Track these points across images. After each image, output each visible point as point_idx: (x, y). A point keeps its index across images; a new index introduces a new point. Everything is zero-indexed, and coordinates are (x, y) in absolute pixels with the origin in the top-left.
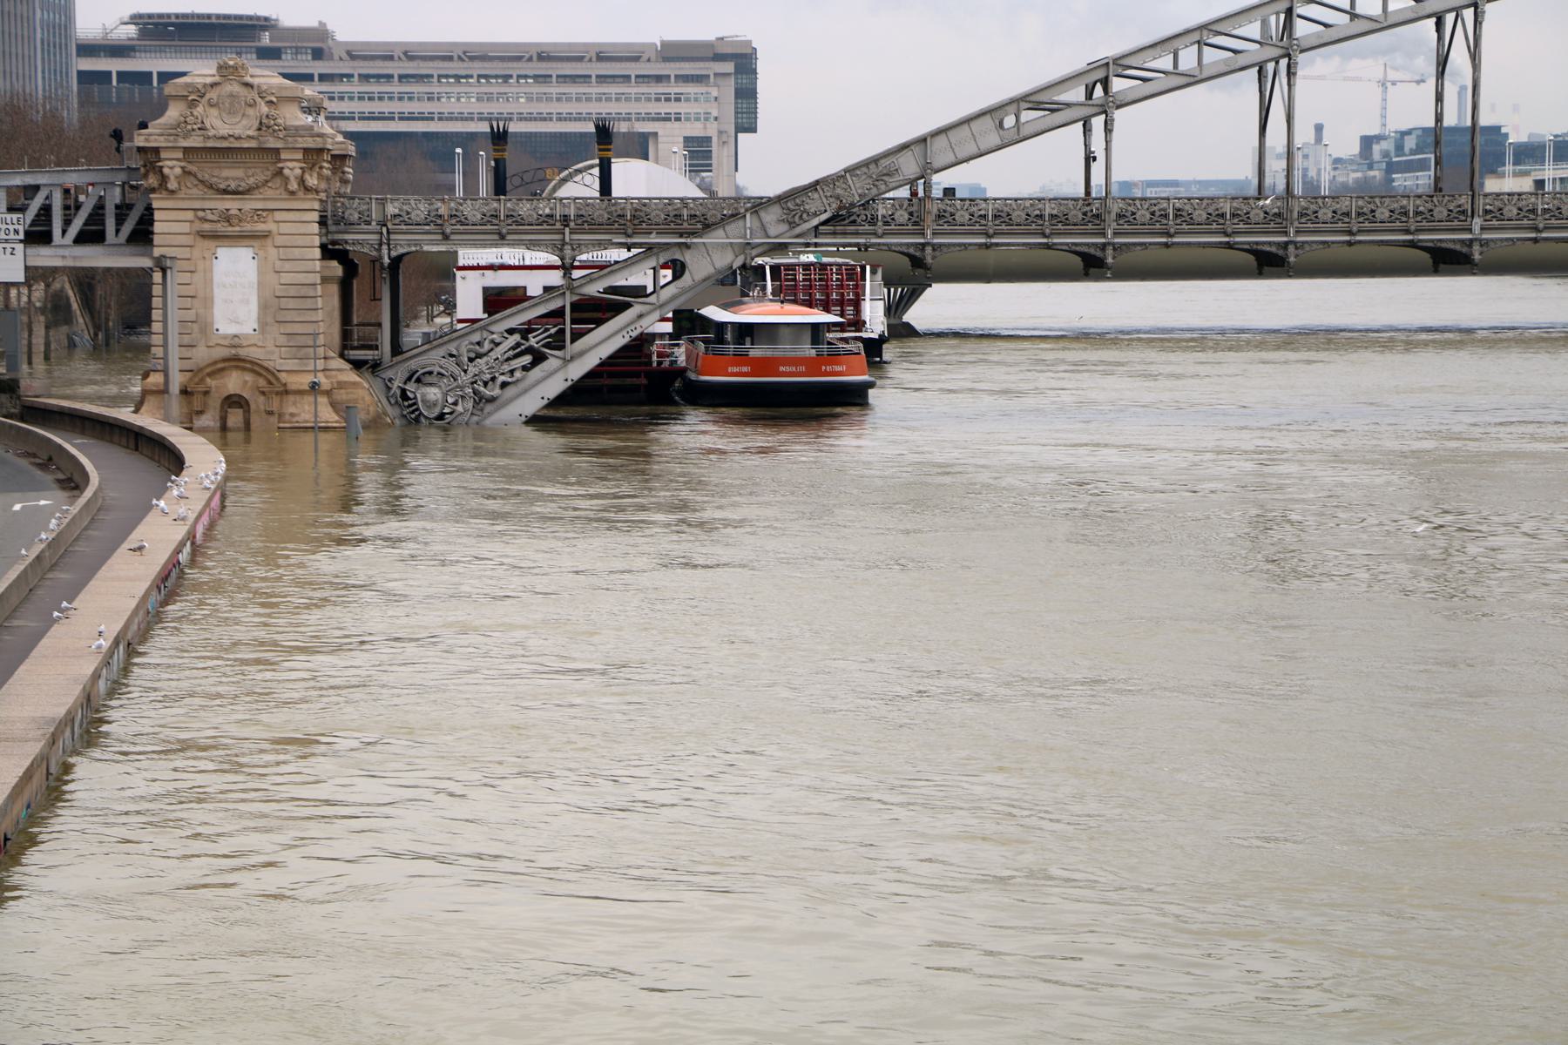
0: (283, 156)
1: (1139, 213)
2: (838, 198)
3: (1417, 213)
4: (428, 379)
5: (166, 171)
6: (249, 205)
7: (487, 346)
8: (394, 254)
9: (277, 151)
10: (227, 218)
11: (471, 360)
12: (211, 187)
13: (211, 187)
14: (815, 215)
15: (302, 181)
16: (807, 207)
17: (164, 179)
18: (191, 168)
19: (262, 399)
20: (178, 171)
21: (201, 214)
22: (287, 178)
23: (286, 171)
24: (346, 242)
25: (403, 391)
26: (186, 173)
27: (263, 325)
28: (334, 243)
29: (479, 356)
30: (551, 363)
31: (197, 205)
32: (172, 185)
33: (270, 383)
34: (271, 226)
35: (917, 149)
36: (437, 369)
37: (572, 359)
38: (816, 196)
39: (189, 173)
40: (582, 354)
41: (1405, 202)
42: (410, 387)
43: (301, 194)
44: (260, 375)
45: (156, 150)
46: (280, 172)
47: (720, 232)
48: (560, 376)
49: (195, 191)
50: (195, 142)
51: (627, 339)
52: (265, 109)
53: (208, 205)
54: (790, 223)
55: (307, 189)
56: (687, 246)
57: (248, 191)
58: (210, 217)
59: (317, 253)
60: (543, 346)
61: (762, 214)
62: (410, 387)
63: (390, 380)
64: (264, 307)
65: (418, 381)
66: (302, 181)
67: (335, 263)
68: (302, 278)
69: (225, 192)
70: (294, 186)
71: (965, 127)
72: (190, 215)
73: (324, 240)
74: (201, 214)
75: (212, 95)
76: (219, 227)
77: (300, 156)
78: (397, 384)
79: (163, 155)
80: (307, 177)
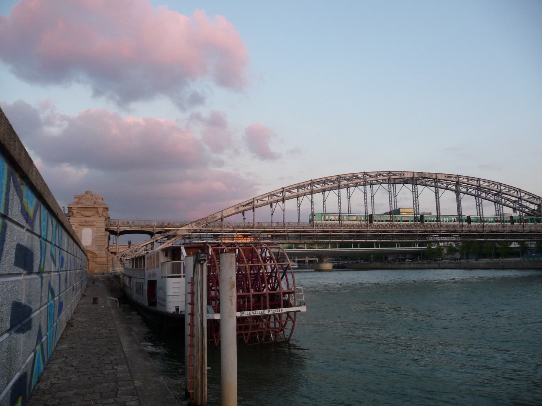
0: (99, 209)
4: (126, 256)
5: (73, 212)
6: (90, 219)
7: (138, 249)
8: (120, 231)
9: (97, 208)
10: (86, 222)
11: (135, 252)
12: (83, 215)
13: (83, 215)
14: (202, 224)
15: (102, 214)
17: (73, 213)
18: (79, 211)
19: (91, 258)
20: (76, 212)
21: (80, 221)
22: (99, 214)
23: (99, 212)
24: (110, 228)
25: (121, 259)
26: (78, 212)
27: (93, 244)
28: (108, 228)
29: (136, 251)
31: (79, 219)
32: (75, 215)
33: (94, 255)
34: (95, 223)
36: (128, 254)
39: (78, 213)
42: (122, 258)
43: (102, 217)
44: (91, 253)
45: (72, 208)
46: (98, 213)
47: (184, 227)
49: (79, 216)
50: (80, 206)
52: (95, 200)
53: (82, 219)
55: (103, 216)
56: (178, 230)
57: (91, 216)
58: (82, 221)
59: (104, 229)
62: (122, 258)
63: (118, 256)
64: (93, 240)
65: (124, 256)
66: (102, 214)
67: (108, 232)
68: (101, 234)
69: (86, 216)
70: (100, 215)
72: (78, 221)
73: (106, 228)
74: (80, 221)
75: (85, 197)
76: (85, 224)
77: (102, 209)
78: (119, 257)
79: (73, 209)
80: (103, 213)
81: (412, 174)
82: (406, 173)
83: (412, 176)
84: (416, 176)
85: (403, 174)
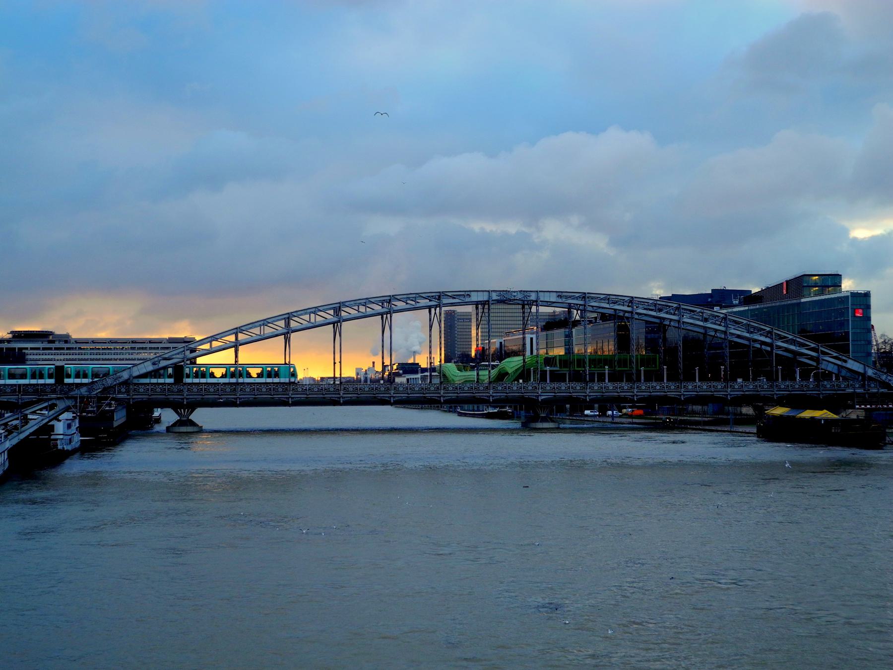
1: (279, 389)
2: (103, 385)
3: (325, 389)
14: (97, 390)
16: (94, 387)
30: (15, 434)
35: (128, 370)
37: (21, 433)
38: (97, 384)
40: (24, 431)
41: (357, 386)
48: (17, 438)
51: (38, 427)
54: (89, 392)
60: (12, 429)
61: (81, 389)
71: (143, 364)
81: (486, 294)
82: (476, 293)
83: (486, 298)
84: (495, 296)
85: (469, 296)
